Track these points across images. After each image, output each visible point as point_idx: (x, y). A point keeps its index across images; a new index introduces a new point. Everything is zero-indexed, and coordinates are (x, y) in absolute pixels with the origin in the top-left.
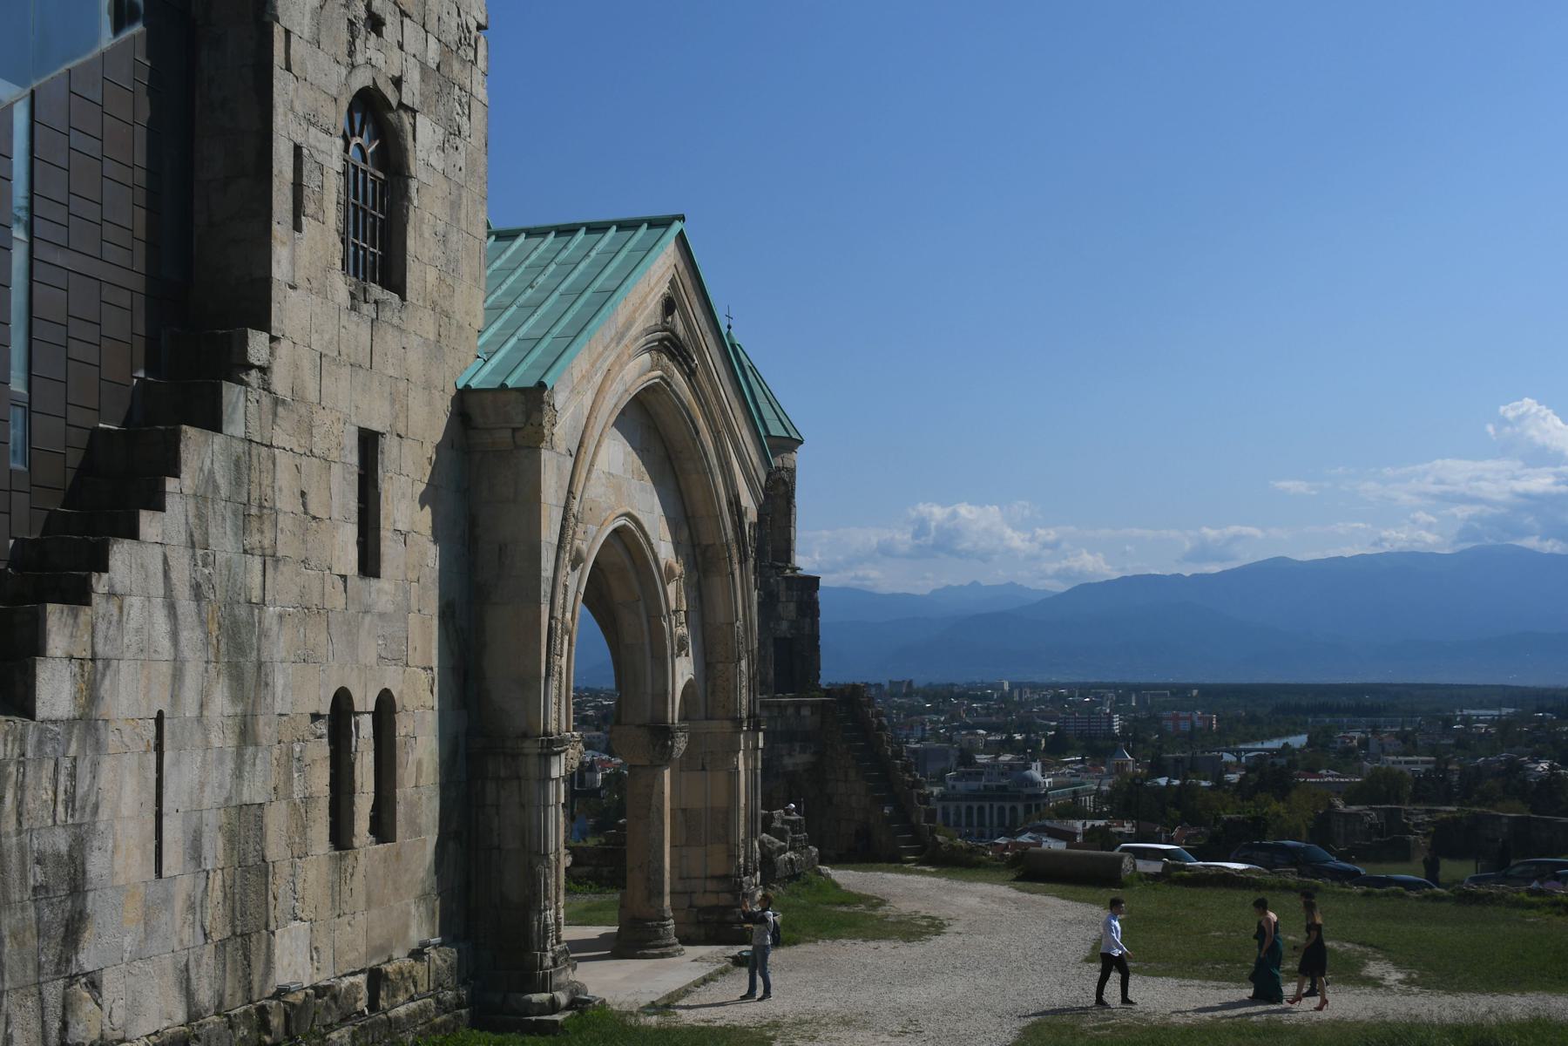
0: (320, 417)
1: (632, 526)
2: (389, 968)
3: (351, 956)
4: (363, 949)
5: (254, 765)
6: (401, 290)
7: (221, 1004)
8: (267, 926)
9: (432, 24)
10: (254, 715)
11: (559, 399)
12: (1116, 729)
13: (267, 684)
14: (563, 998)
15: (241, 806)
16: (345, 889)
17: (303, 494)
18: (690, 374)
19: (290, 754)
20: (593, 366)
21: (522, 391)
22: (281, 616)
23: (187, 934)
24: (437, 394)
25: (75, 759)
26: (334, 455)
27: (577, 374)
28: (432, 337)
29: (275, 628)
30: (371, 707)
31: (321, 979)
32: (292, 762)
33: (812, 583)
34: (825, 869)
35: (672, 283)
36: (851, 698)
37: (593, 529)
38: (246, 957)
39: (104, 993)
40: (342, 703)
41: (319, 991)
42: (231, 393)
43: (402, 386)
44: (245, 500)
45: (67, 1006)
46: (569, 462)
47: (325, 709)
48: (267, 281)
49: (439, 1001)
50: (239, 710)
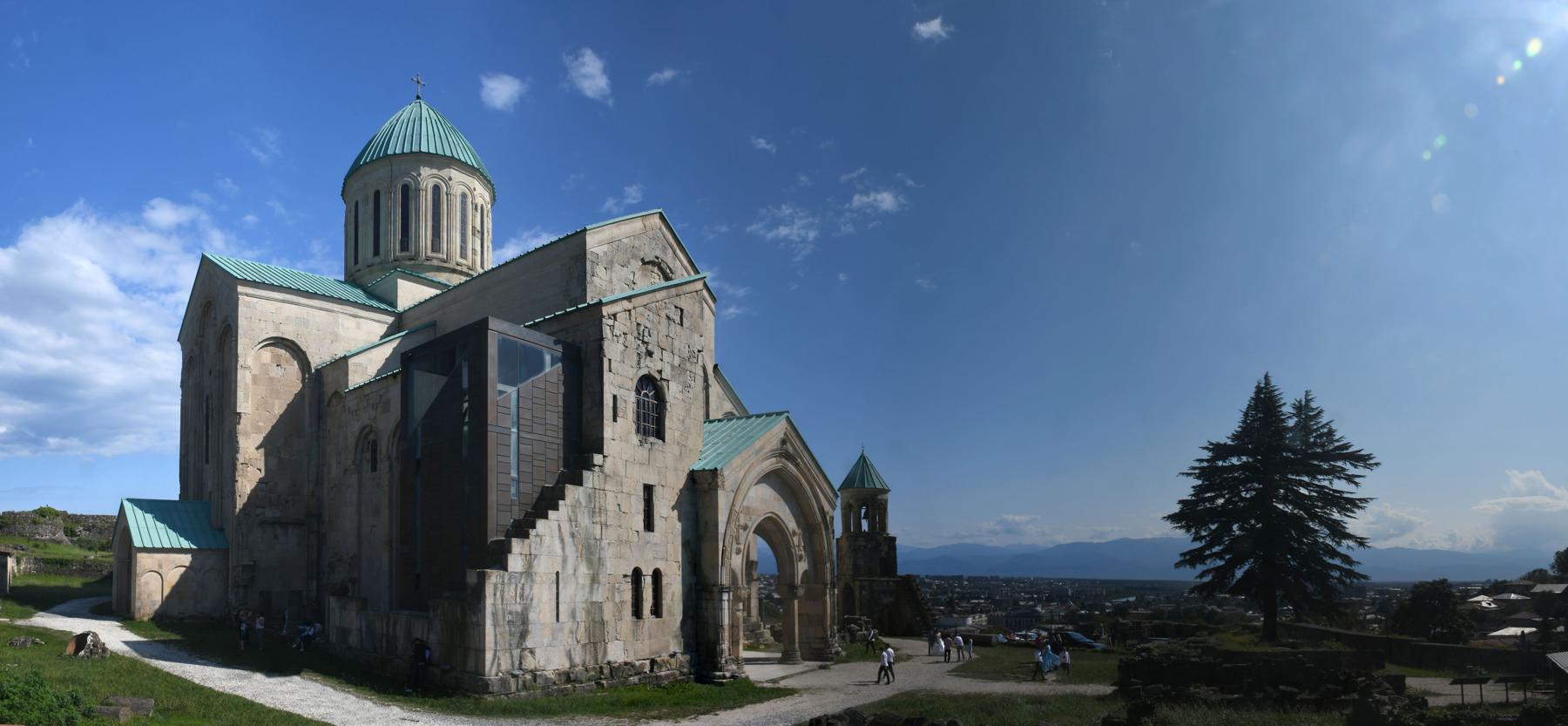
0: (625, 480)
1: (774, 516)
2: (658, 659)
3: (642, 654)
4: (648, 652)
6: (664, 441)
7: (584, 663)
8: (604, 641)
9: (676, 351)
10: (598, 574)
11: (726, 473)
12: (1070, 594)
14: (728, 674)
16: (640, 632)
17: (619, 505)
18: (797, 465)
19: (614, 587)
20: (743, 462)
21: (711, 470)
22: (609, 544)
23: (570, 641)
24: (680, 473)
25: (523, 584)
26: (632, 492)
27: (734, 465)
28: (678, 454)
29: (606, 547)
30: (651, 573)
31: (628, 660)
32: (614, 590)
33: (894, 539)
34: (880, 637)
35: (785, 434)
36: (908, 579)
37: (754, 517)
38: (596, 650)
40: (637, 574)
41: (626, 664)
42: (586, 474)
43: (664, 470)
45: (521, 658)
46: (733, 495)
47: (630, 573)
48: (602, 439)
49: (681, 672)
50: (591, 572)
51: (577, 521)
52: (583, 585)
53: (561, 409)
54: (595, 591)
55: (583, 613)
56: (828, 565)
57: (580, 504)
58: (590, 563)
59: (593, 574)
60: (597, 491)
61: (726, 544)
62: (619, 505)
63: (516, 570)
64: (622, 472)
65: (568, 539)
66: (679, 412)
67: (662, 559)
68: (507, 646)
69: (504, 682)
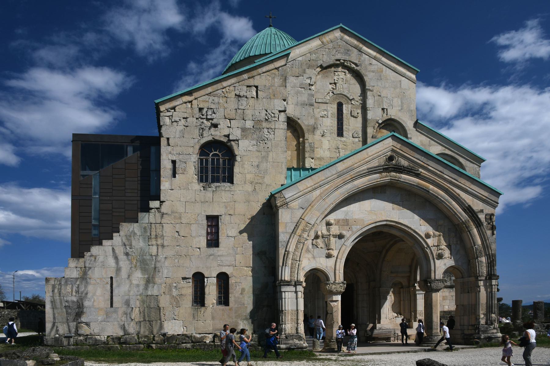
5: (153, 287)
6: (231, 181)
10: (153, 277)
13: (159, 271)
15: (147, 296)
17: (177, 232)
22: (166, 258)
23: (123, 319)
39: (91, 326)
44: (149, 235)
50: (146, 276)
51: (131, 245)
52: (138, 286)
53: (139, 178)
54: (150, 289)
55: (138, 303)
56: (483, 259)
57: (135, 234)
58: (144, 270)
59: (148, 278)
60: (153, 225)
61: (292, 248)
62: (177, 232)
63: (71, 277)
64: (181, 210)
65: (122, 257)
66: (252, 160)
67: (229, 266)
68: (65, 320)
69: (56, 339)
